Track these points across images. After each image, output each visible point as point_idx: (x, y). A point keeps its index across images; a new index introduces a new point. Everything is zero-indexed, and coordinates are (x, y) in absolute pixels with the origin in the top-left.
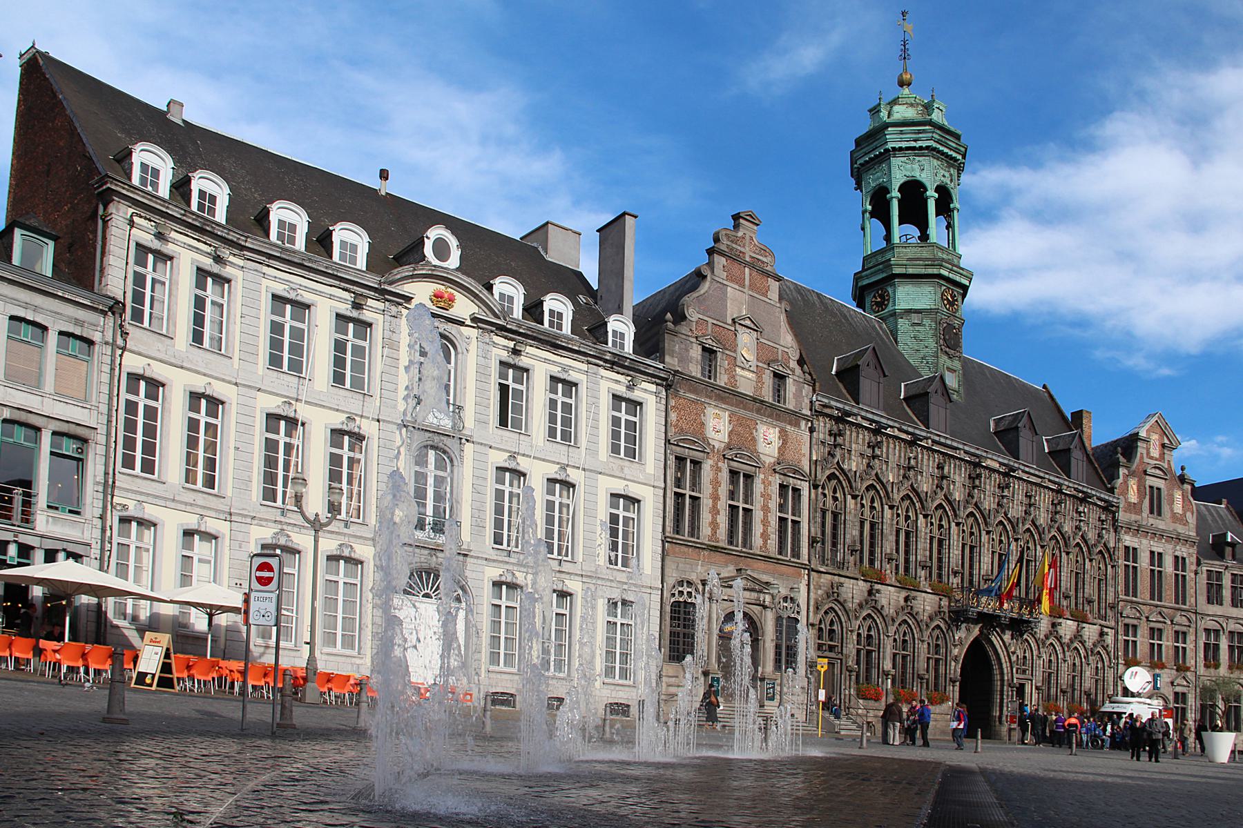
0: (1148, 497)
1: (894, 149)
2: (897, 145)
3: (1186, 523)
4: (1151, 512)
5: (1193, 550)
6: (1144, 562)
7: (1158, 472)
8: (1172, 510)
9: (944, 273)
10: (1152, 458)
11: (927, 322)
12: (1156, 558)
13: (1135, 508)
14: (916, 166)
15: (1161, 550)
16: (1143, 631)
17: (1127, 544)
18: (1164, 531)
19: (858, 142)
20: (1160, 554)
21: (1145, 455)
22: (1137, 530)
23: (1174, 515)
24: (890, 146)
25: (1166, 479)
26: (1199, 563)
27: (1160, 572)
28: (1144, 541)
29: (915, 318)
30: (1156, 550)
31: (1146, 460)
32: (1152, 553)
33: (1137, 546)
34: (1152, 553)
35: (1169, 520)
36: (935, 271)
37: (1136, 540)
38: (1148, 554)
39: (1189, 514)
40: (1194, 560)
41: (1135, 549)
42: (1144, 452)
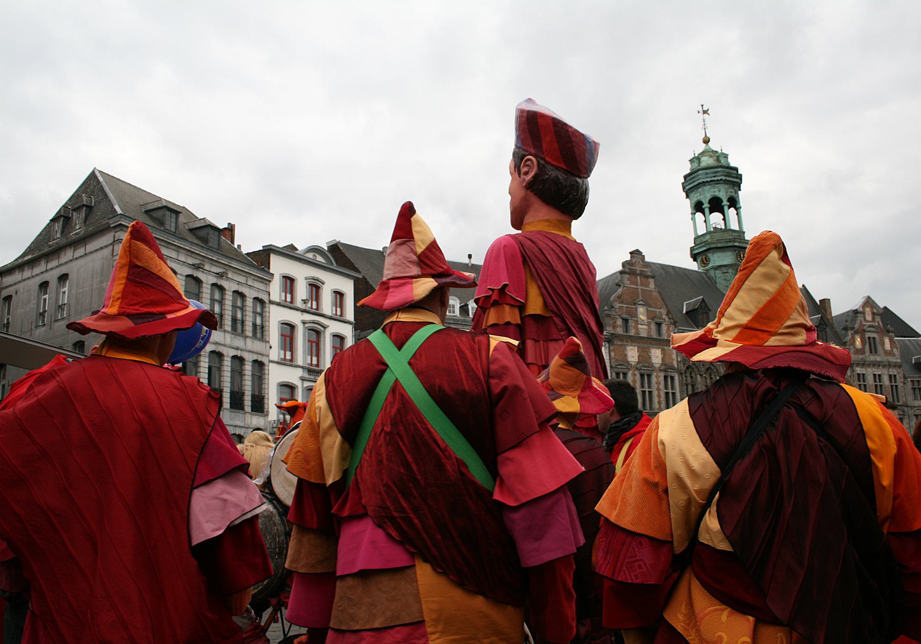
0: (868, 345)
2: (705, 180)
3: (894, 355)
4: (871, 352)
7: (872, 329)
8: (884, 349)
9: (736, 244)
10: (867, 321)
11: (730, 271)
13: (861, 351)
15: (880, 373)
17: (858, 372)
19: (685, 177)
20: (879, 375)
21: (863, 321)
22: (863, 364)
24: (700, 181)
25: (878, 332)
26: (905, 378)
27: (881, 386)
28: (869, 370)
32: (875, 375)
33: (864, 372)
34: (875, 375)
35: (883, 355)
36: (731, 244)
37: (864, 369)
38: (872, 376)
39: (895, 350)
40: (901, 375)
41: (863, 375)
42: (862, 319)
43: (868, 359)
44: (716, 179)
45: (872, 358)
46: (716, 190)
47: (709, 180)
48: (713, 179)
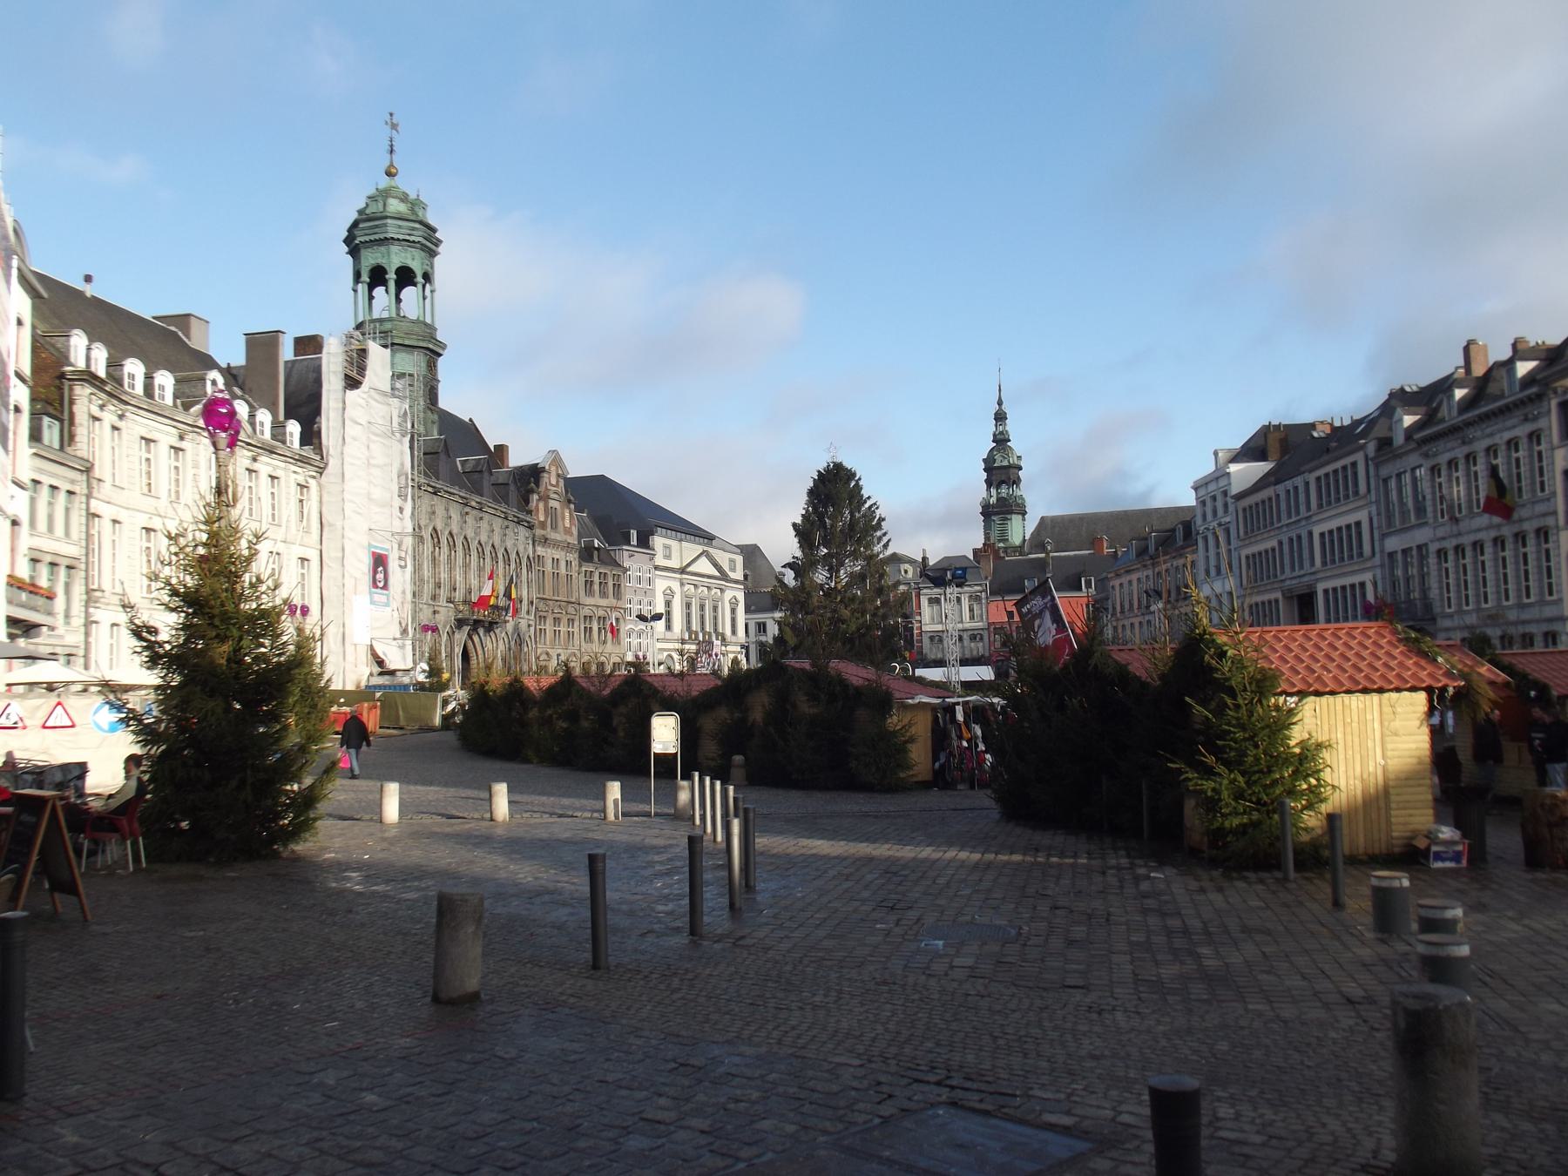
1: (392, 238)
2: (396, 236)
3: (571, 535)
5: (576, 555)
6: (549, 567)
9: (431, 346)
12: (556, 562)
13: (543, 525)
14: (409, 255)
16: (549, 621)
23: (565, 527)
26: (580, 566)
28: (549, 550)
30: (556, 557)
31: (549, 487)
36: (425, 345)
39: (573, 528)
43: (548, 537)
44: (411, 238)
45: (553, 536)
47: (401, 237)
48: (408, 238)
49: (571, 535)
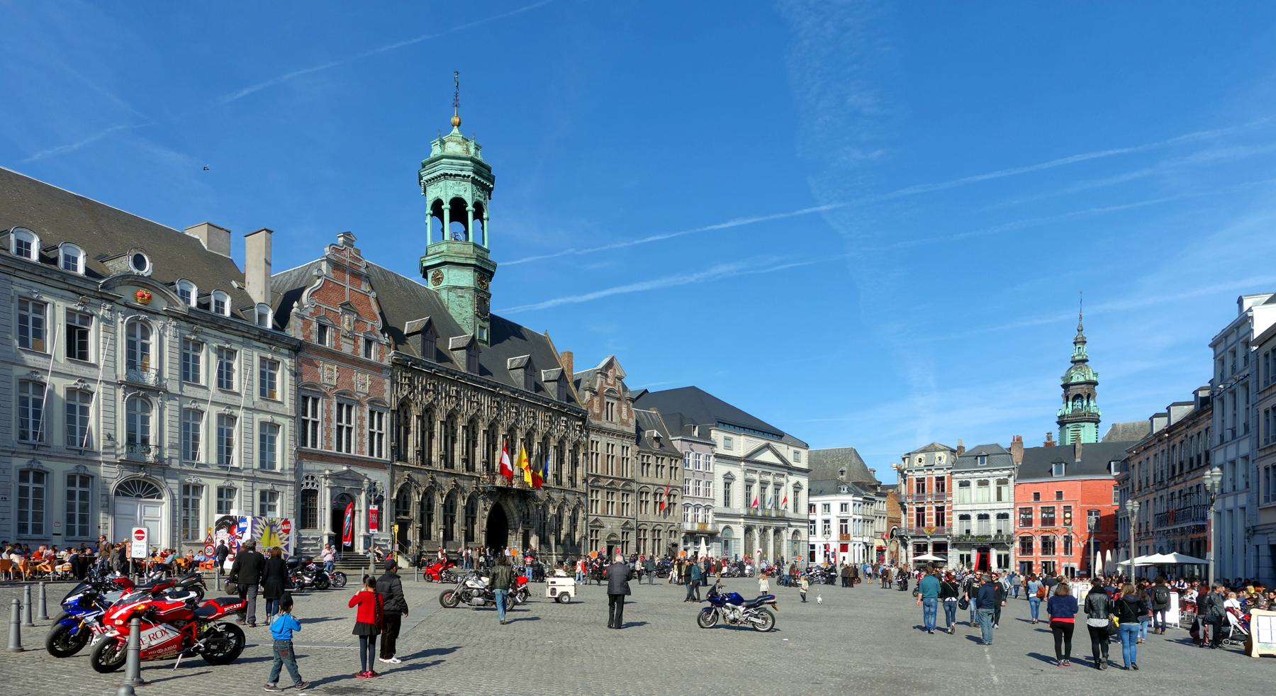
2: (449, 172)
3: (629, 426)
10: (609, 384)
11: (467, 295)
13: (598, 417)
15: (614, 443)
18: (615, 431)
21: (604, 383)
22: (600, 430)
29: (460, 292)
30: (611, 442)
31: (605, 386)
43: (604, 426)
44: (463, 173)
45: (607, 425)
46: (462, 188)
48: (459, 173)
49: (629, 426)
